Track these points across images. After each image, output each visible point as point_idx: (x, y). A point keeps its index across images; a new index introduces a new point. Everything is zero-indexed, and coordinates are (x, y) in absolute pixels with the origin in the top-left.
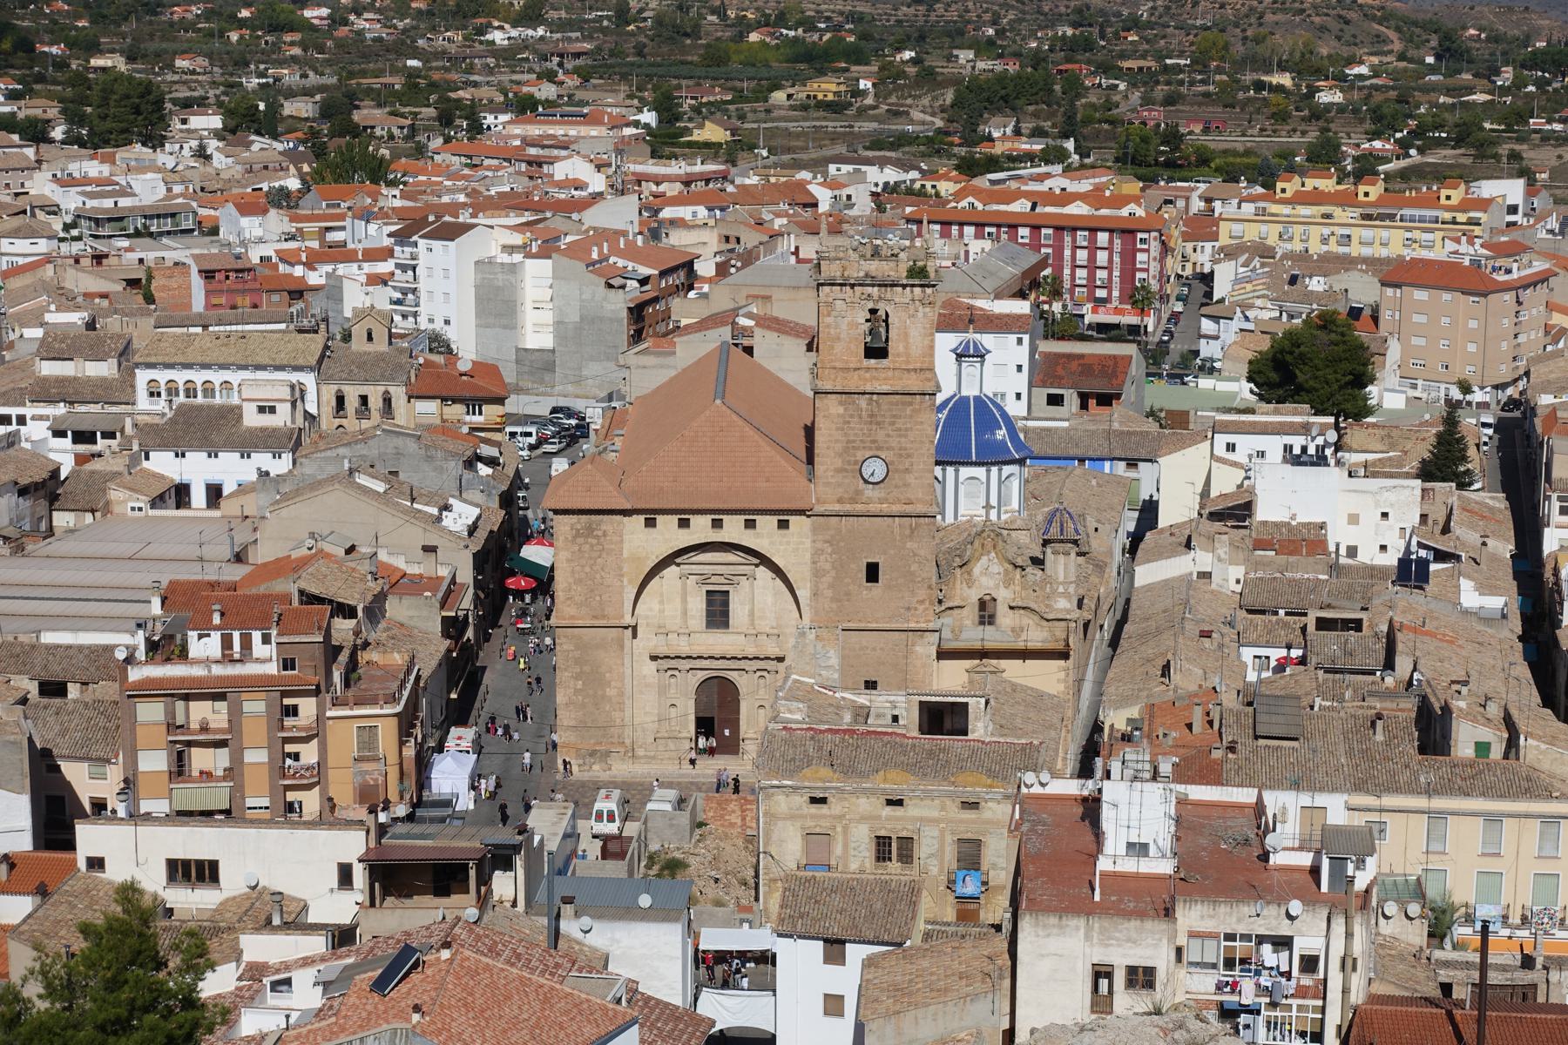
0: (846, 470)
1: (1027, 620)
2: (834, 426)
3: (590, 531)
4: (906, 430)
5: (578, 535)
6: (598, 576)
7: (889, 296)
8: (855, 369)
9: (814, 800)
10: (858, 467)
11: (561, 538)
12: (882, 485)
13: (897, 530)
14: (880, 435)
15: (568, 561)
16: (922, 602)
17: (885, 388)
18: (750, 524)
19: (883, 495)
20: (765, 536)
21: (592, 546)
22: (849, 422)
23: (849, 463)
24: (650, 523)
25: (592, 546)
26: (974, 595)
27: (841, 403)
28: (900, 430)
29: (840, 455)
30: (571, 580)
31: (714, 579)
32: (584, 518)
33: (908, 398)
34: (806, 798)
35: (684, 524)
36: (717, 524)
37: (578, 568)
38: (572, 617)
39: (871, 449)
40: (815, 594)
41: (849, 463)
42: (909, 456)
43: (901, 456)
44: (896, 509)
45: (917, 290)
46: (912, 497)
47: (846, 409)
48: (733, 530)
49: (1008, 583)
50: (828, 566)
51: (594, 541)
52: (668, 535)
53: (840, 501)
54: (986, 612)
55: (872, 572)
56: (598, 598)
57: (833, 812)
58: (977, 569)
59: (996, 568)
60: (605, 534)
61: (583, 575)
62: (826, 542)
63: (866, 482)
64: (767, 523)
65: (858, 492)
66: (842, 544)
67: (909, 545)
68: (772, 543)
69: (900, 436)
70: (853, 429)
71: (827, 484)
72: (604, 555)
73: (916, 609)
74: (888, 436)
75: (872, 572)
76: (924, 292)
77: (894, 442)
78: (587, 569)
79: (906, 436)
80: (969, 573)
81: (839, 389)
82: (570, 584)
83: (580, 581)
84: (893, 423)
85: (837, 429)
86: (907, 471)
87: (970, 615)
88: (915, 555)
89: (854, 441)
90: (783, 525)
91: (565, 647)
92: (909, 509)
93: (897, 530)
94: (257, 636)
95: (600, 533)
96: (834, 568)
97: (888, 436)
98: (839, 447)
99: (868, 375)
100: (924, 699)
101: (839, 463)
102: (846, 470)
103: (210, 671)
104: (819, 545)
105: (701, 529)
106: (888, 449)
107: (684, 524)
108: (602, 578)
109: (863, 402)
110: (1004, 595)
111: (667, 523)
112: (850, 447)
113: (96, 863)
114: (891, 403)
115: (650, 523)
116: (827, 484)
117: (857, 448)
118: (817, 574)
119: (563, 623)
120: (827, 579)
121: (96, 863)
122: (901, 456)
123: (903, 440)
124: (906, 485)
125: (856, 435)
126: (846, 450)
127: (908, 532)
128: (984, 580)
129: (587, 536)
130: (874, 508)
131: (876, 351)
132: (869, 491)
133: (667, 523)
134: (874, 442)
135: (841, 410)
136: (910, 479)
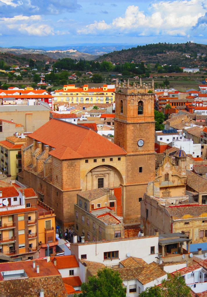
0: (134, 144)
1: (176, 179)
2: (131, 132)
3: (72, 165)
4: (148, 132)
5: (69, 166)
7: (144, 98)
8: (136, 117)
9: (186, 223)
10: (137, 143)
11: (64, 167)
12: (142, 147)
13: (146, 158)
14: (142, 134)
15: (66, 173)
16: (152, 176)
17: (143, 122)
18: (111, 160)
19: (143, 149)
20: (115, 163)
22: (135, 131)
23: (135, 142)
24: (87, 161)
26: (164, 173)
27: (133, 126)
28: (146, 132)
29: (133, 140)
30: (67, 179)
31: (100, 176)
32: (70, 161)
33: (149, 124)
34: (184, 223)
35: (95, 161)
36: (103, 160)
38: (67, 189)
39: (140, 138)
40: (127, 177)
41: (135, 142)
42: (149, 139)
43: (147, 139)
44: (146, 152)
45: (150, 96)
46: (149, 149)
47: (134, 128)
48: (107, 162)
49: (171, 170)
50: (130, 169)
51: (73, 168)
52: (91, 164)
53: (133, 152)
54: (167, 176)
55: (141, 170)
56: (74, 183)
57: (190, 226)
58: (165, 166)
59: (169, 166)
60: (76, 165)
62: (130, 163)
63: (139, 146)
64: (115, 159)
65: (137, 149)
66: (133, 163)
67: (149, 162)
68: (116, 164)
69: (147, 134)
70: (136, 133)
71: (130, 147)
72: (75, 171)
73: (151, 178)
74: (144, 134)
75: (141, 170)
76: (152, 97)
77: (145, 135)
78: (71, 175)
79: (148, 134)
80: (163, 168)
81: (132, 122)
82: (66, 180)
83: (69, 178)
84: (145, 131)
85: (132, 133)
86: (148, 143)
87: (163, 179)
88: (151, 164)
89: (136, 136)
90: (119, 159)
91: (65, 197)
92: (149, 152)
93: (146, 158)
94: (12, 199)
95: (74, 165)
97: (144, 134)
98: (132, 138)
99: (139, 119)
100: (203, 195)
101: (132, 142)
102: (134, 144)
103: (7, 209)
104: (128, 164)
105: (99, 162)
106: (144, 137)
107: (95, 161)
109: (138, 126)
110: (170, 173)
111: (91, 161)
112: (135, 138)
113: (84, 256)
114: (144, 126)
115: (87, 161)
116: (130, 147)
117: (136, 138)
118: (127, 171)
119: (66, 190)
120: (130, 172)
121: (84, 256)
122: (147, 139)
123: (147, 135)
124: (148, 146)
125: (136, 134)
126: (134, 138)
127: (149, 159)
128: (166, 169)
129: (71, 166)
130: (141, 153)
131: (140, 113)
132: (140, 149)
133: (91, 161)
134: (140, 136)
135: (133, 128)
136: (149, 145)
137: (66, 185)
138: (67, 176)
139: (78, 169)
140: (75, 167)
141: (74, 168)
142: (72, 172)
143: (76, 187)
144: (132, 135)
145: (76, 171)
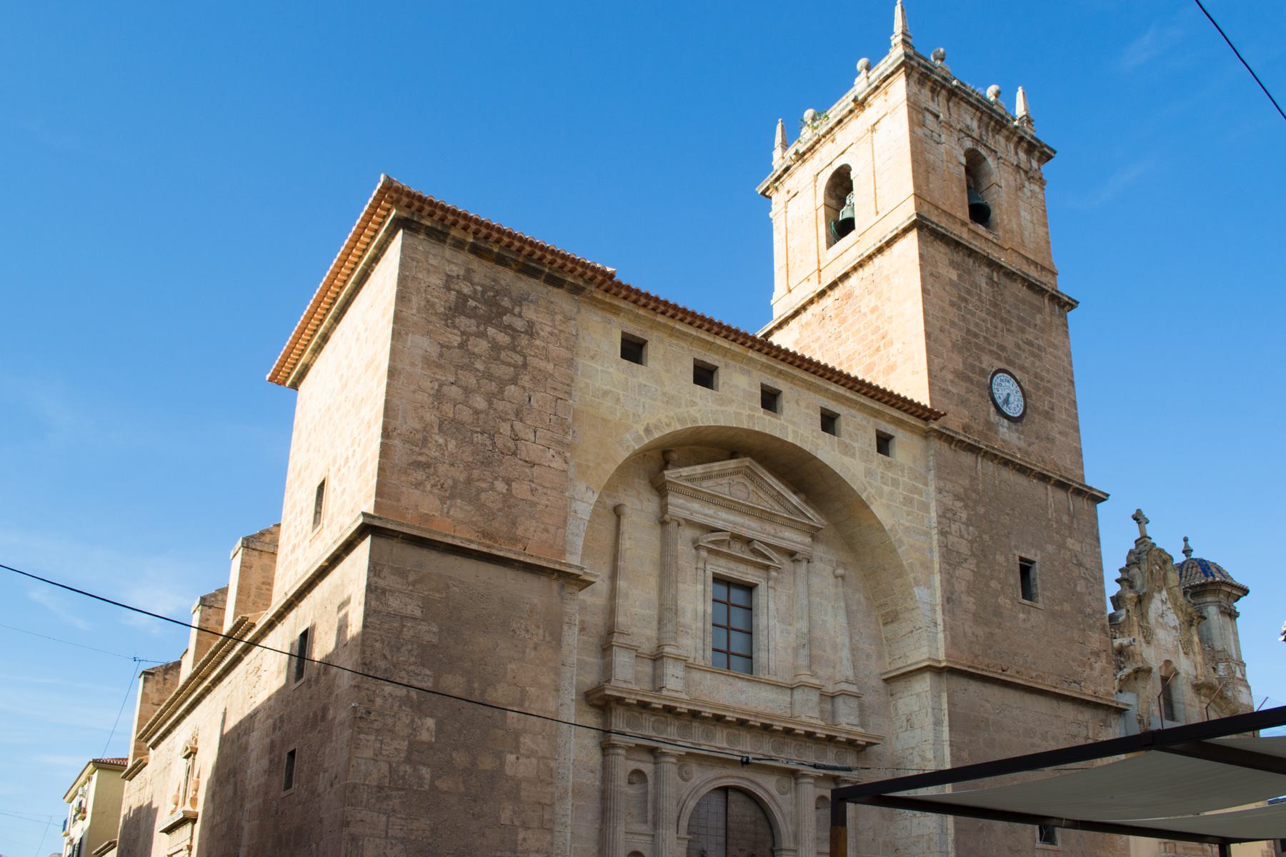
6: (505, 428)
14: (1009, 341)
15: (428, 361)
21: (496, 347)
22: (965, 300)
25: (496, 347)
37: (454, 392)
50: (964, 548)
51: (503, 339)
56: (501, 486)
61: (466, 415)
72: (525, 380)
78: (479, 402)
83: (458, 425)
89: (976, 335)
95: (519, 324)
96: (973, 555)
98: (956, 334)
108: (516, 439)
137: (420, 475)
138: (439, 396)
139: (550, 367)
140: (524, 341)
141: (513, 348)
142: (489, 376)
143: (520, 532)
144: (953, 313)
145: (534, 378)
